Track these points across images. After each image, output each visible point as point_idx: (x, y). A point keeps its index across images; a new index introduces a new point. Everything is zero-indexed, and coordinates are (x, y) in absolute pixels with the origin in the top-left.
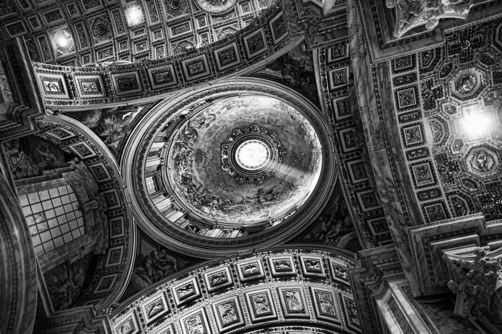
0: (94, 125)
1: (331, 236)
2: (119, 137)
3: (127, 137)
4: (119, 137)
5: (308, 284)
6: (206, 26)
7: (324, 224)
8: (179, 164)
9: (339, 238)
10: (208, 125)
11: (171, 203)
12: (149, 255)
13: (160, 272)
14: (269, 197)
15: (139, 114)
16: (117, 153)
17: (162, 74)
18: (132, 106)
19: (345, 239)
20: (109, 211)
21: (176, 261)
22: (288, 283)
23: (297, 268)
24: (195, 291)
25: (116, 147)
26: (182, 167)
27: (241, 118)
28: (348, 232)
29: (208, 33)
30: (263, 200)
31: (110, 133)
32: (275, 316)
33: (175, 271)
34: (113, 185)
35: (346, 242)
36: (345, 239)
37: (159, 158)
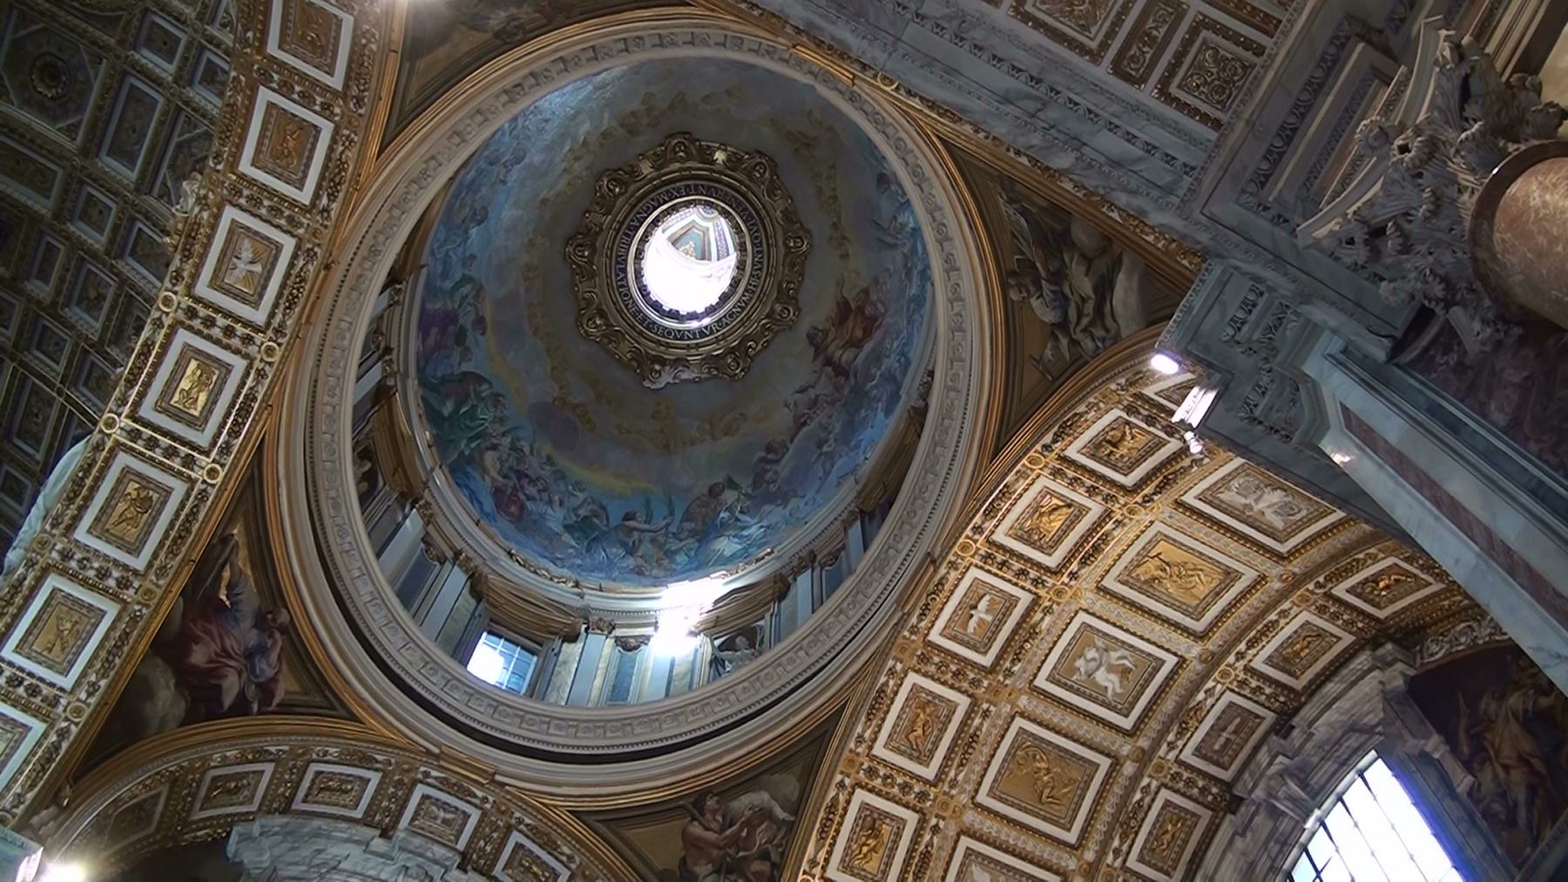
0: (182, 706)
1: (1085, 321)
2: (274, 656)
3: (290, 631)
4: (274, 656)
5: (1163, 504)
6: (184, 38)
7: (1035, 303)
8: (522, 507)
9: (1107, 309)
10: (480, 322)
11: (611, 642)
12: (683, 853)
13: (757, 866)
14: (854, 328)
15: (250, 547)
16: (318, 699)
17: (185, 384)
18: (210, 547)
19: (1124, 293)
20: (464, 855)
21: (765, 796)
22: (1111, 550)
23: (1092, 491)
24: (893, 818)
25: (295, 687)
26: (542, 508)
27: (544, 201)
28: (1117, 264)
29: (208, 54)
30: (848, 355)
31: (240, 674)
32: (1171, 661)
33: (791, 828)
34: (400, 783)
35: (1133, 300)
36: (1124, 293)
37: (448, 565)
